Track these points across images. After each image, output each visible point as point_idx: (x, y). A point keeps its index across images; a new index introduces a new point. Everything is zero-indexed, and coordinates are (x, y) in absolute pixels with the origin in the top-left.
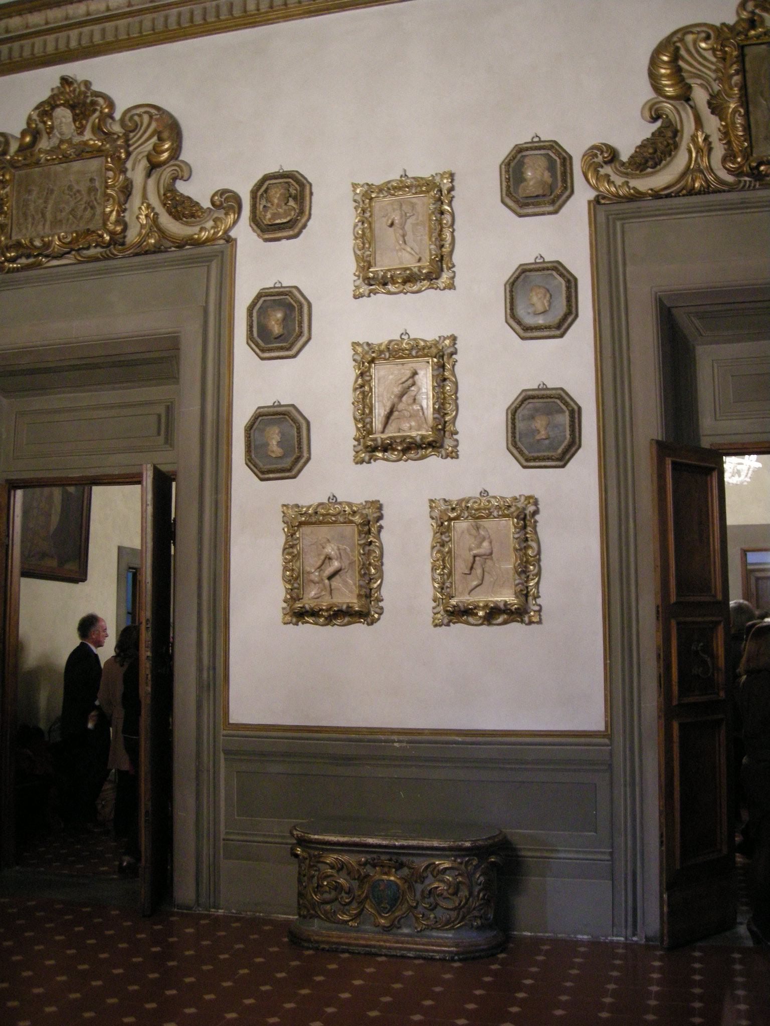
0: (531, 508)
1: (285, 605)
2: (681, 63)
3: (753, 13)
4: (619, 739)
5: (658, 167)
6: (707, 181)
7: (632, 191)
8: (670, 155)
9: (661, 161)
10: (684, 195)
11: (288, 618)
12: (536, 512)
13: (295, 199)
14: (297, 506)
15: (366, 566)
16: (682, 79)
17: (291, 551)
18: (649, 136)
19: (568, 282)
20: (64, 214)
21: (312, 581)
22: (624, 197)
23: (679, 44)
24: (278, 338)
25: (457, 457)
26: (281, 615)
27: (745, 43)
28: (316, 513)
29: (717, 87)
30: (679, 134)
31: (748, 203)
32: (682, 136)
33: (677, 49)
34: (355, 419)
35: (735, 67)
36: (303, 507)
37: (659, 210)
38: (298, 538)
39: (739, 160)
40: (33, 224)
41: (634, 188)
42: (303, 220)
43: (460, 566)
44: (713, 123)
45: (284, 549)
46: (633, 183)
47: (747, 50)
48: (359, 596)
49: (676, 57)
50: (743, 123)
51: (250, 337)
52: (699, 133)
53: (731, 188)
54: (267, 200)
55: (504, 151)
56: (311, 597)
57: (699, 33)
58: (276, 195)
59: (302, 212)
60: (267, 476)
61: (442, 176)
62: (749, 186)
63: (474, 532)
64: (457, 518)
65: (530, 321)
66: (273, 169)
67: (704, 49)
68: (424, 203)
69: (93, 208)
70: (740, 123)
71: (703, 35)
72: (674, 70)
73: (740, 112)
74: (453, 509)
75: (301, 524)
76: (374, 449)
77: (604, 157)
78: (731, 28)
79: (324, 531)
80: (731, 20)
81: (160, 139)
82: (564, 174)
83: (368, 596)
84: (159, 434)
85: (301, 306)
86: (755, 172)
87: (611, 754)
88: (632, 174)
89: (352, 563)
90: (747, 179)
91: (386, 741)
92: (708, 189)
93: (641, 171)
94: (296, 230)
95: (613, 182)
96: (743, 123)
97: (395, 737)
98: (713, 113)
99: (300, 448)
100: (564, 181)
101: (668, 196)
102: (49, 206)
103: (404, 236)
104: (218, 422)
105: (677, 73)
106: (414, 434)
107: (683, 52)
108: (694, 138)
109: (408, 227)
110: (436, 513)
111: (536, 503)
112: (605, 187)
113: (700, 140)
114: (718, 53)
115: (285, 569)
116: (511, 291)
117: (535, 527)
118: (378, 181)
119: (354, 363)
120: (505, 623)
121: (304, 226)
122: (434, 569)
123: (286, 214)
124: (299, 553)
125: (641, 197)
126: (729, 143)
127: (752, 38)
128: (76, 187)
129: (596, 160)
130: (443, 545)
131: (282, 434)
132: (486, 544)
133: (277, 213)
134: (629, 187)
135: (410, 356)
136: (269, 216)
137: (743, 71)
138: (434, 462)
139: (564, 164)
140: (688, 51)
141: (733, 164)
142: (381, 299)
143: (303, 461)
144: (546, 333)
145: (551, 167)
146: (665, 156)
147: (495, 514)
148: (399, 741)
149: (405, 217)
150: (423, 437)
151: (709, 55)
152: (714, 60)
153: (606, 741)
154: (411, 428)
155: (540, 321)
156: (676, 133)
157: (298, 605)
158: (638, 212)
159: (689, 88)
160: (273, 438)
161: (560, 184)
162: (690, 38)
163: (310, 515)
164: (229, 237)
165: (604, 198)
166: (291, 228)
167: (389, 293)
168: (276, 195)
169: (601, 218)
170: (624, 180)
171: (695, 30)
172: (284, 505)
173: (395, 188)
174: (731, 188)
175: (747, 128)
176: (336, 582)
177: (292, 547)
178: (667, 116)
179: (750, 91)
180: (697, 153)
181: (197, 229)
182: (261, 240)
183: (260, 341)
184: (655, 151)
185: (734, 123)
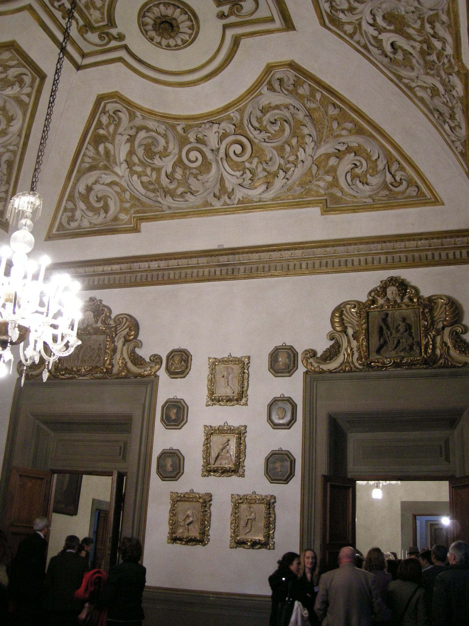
0: (273, 500)
1: (169, 535)
2: (343, 317)
3: (374, 297)
6: (351, 368)
8: (337, 356)
9: (333, 358)
11: (169, 541)
12: (275, 502)
13: (185, 361)
14: (177, 493)
15: (203, 521)
16: (343, 324)
17: (173, 512)
18: (328, 347)
19: (293, 406)
20: (87, 358)
21: (181, 526)
22: (317, 372)
23: (343, 309)
24: (174, 421)
25: (244, 477)
26: (167, 539)
28: (184, 496)
33: (343, 311)
34: (203, 458)
36: (179, 493)
38: (176, 507)
40: (73, 360)
41: (322, 369)
42: (187, 371)
43: (242, 523)
44: (354, 344)
45: (170, 511)
46: (321, 366)
48: (200, 533)
51: (162, 419)
53: (361, 370)
55: (271, 349)
56: (180, 532)
58: (177, 359)
59: (187, 368)
60: (165, 479)
61: (245, 357)
63: (249, 509)
64: (242, 503)
65: (277, 421)
66: (176, 347)
68: (236, 369)
69: (100, 357)
71: (353, 306)
74: (241, 499)
75: (178, 501)
76: (210, 471)
79: (187, 505)
81: (130, 330)
82: (294, 361)
83: (204, 533)
84: (120, 455)
85: (184, 408)
86: (370, 365)
89: (198, 519)
91: (208, 597)
94: (184, 375)
97: (211, 595)
99: (180, 468)
100: (294, 364)
101: (335, 372)
102: (81, 353)
103: (228, 382)
104: (146, 454)
105: (342, 320)
106: (226, 466)
107: (345, 312)
108: (346, 350)
109: (230, 378)
110: (234, 500)
111: (275, 498)
112: (309, 367)
115: (170, 519)
116: (270, 409)
117: (274, 509)
118: (219, 357)
119: (204, 434)
120: (259, 548)
121: (188, 373)
122: (231, 524)
123: (181, 368)
124: (176, 513)
126: (360, 352)
128: (93, 347)
129: (307, 356)
130: (236, 514)
131: (173, 461)
132: (253, 514)
133: (177, 366)
134: (319, 368)
135: (227, 433)
136: (173, 368)
137: (368, 322)
138: (234, 478)
139: (294, 357)
140: (347, 312)
142: (217, 407)
143: (180, 474)
144: (283, 427)
145: (289, 357)
147: (258, 502)
148: (213, 597)
149: (229, 374)
150: (230, 468)
151: (355, 314)
154: (225, 463)
155: (281, 422)
157: (174, 535)
159: (346, 328)
160: (169, 463)
161: (292, 365)
163: (182, 497)
164: (156, 375)
165: (309, 372)
166: (182, 374)
167: (220, 405)
168: (177, 359)
169: (308, 380)
170: (318, 365)
172: (171, 492)
173: (226, 361)
174: (361, 370)
175: (368, 347)
176: (191, 527)
177: (173, 510)
178: (337, 339)
179: (370, 330)
181: (143, 370)
182: (169, 378)
183: (166, 421)
185: (362, 344)
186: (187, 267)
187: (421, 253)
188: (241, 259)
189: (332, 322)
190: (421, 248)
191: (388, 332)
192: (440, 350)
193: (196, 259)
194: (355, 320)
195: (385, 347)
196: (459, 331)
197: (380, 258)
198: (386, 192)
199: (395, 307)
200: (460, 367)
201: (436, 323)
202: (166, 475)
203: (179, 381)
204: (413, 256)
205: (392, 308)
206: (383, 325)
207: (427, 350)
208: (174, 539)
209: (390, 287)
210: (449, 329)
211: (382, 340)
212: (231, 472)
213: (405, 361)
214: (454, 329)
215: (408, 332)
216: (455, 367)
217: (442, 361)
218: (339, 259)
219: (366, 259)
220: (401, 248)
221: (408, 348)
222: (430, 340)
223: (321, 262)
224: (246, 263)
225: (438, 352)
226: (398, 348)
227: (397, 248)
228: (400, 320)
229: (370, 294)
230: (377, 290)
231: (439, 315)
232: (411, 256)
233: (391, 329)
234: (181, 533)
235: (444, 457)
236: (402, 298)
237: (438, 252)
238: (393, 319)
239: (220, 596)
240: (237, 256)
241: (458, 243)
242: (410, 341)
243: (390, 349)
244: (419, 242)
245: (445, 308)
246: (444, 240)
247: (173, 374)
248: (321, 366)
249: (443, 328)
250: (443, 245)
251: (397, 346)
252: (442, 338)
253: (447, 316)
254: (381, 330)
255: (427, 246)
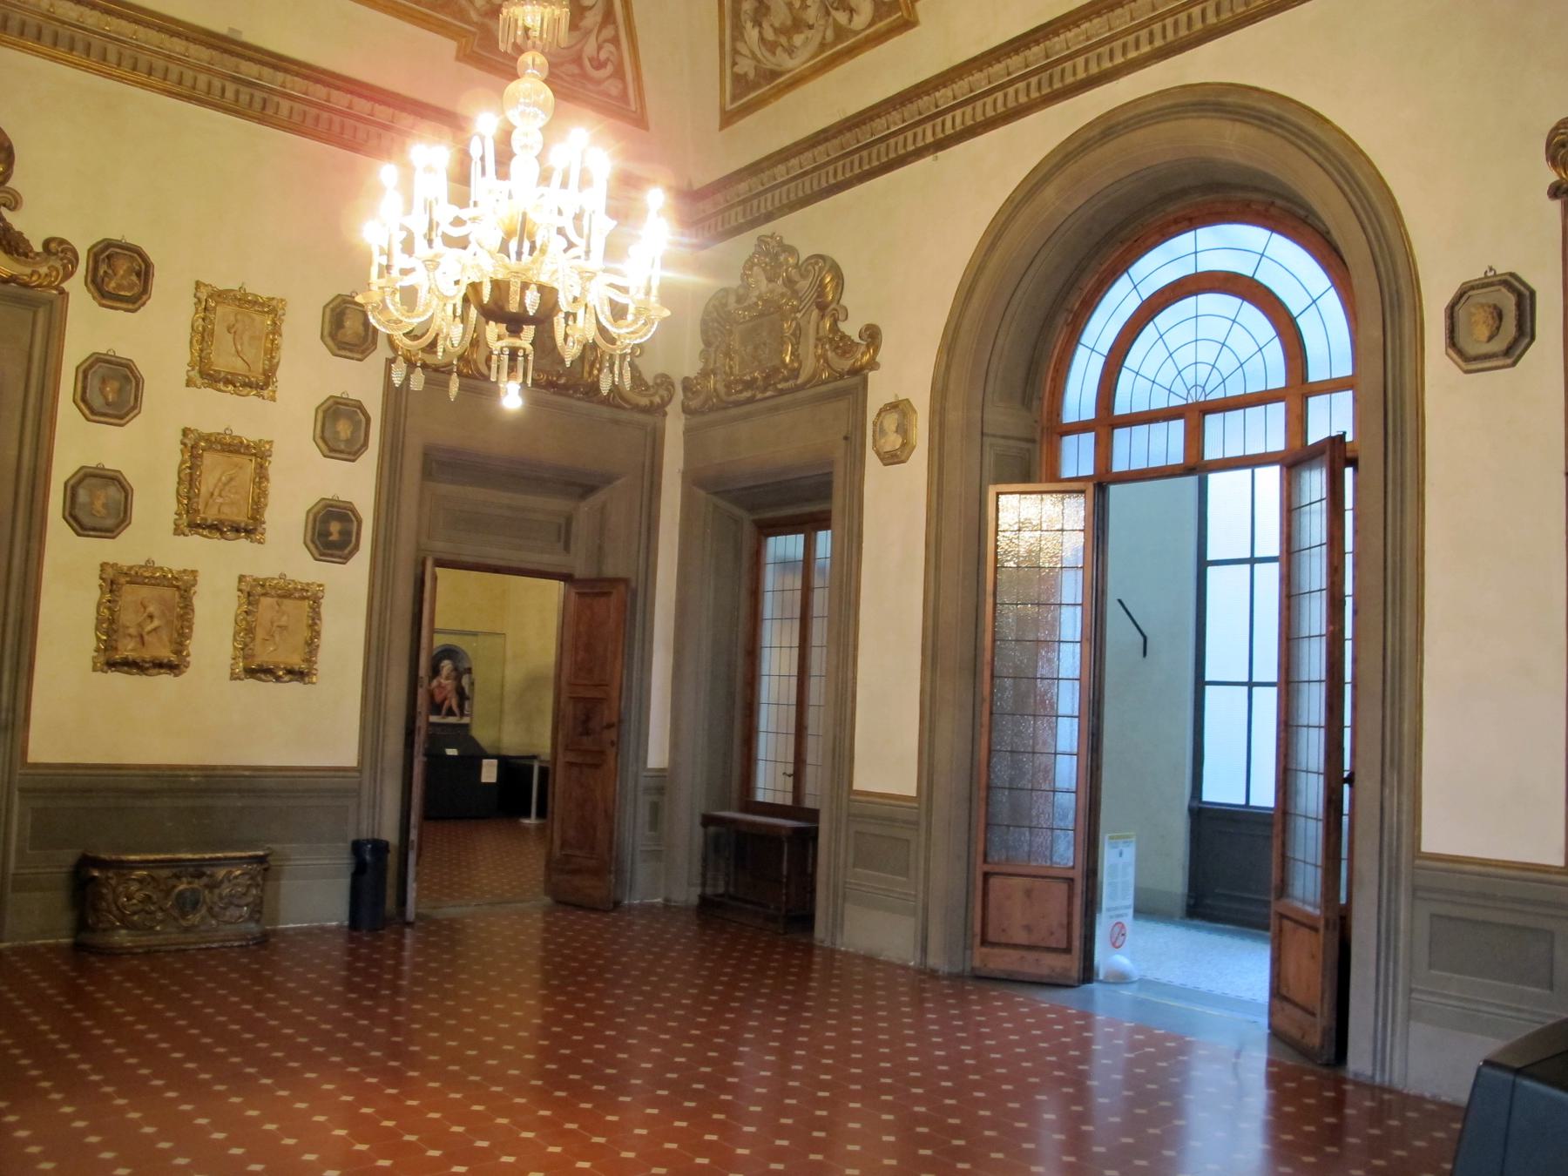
4: (367, 773)
13: (138, 274)
43: (260, 634)
54: (109, 266)
56: (128, 649)
60: (86, 533)
63: (277, 607)
79: (144, 592)
87: (360, 784)
101: (443, 372)
136: (113, 284)
138: (243, 544)
148: (196, 776)
153: (357, 774)
166: (134, 303)
181: (28, 271)
182: (95, 304)
186: (157, 53)
188: (289, 85)
193: (184, 43)
198: (576, 70)
202: (80, 525)
203: (119, 316)
208: (113, 662)
212: (204, 529)
224: (297, 97)
234: (132, 650)
235: (562, 543)
239: (208, 773)
240: (280, 76)
247: (103, 292)
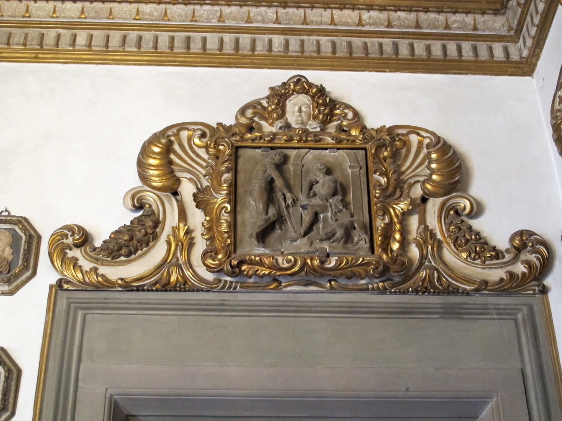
2: (172, 156)
3: (251, 119)
5: (133, 256)
6: (184, 276)
7: (100, 279)
8: (147, 245)
9: (136, 250)
10: (157, 290)
16: (172, 172)
19: (9, 371)
22: (92, 284)
23: (173, 138)
27: (240, 144)
29: (206, 183)
30: (160, 225)
31: (227, 305)
32: (163, 229)
33: (170, 143)
35: (226, 164)
37: (127, 303)
39: (220, 256)
41: (103, 276)
46: (103, 270)
47: (241, 152)
49: (168, 149)
50: (229, 220)
52: (181, 225)
53: (210, 287)
57: (194, 130)
62: (230, 287)
67: (199, 147)
70: (225, 220)
71: (199, 132)
72: (164, 161)
73: (227, 208)
77: (74, 239)
78: (228, 129)
80: (229, 121)
82: (28, 252)
86: (237, 270)
88: (103, 260)
90: (229, 279)
92: (184, 285)
93: (113, 258)
95: (80, 267)
96: (229, 220)
98: (198, 206)
100: (26, 260)
101: (139, 289)
107: (176, 147)
112: (70, 274)
113: (182, 233)
114: (211, 150)
125: (108, 287)
127: (247, 140)
129: (65, 241)
137: (235, 171)
139: (29, 242)
141: (213, 260)
146: (141, 245)
151: (202, 152)
152: (206, 157)
156: (157, 223)
158: (104, 303)
159: (178, 181)
161: (20, 262)
162: (184, 134)
165: (68, 282)
169: (62, 305)
171: (191, 127)
174: (210, 287)
175: (233, 225)
178: (150, 206)
180: (177, 245)
184: (131, 239)
185: (219, 218)
187: (367, 40)
189: (141, 165)
190: (367, 28)
191: (288, 195)
192: (419, 246)
194: (201, 165)
195: (279, 231)
196: (465, 208)
197: (270, 41)
199: (307, 141)
200: (467, 293)
201: (406, 186)
204: (350, 44)
205: (299, 141)
206: (275, 174)
207: (388, 244)
209: (295, 95)
210: (439, 201)
211: (272, 211)
213: (333, 264)
214: (452, 202)
215: (339, 197)
216: (456, 291)
217: (423, 274)
218: (172, 34)
219: (237, 40)
220: (321, 23)
221: (339, 234)
222: (396, 220)
223: (125, 37)
225: (414, 252)
226: (313, 233)
227: (312, 22)
228: (320, 170)
229: (242, 111)
230: (260, 104)
231: (414, 171)
232: (344, 44)
233: (297, 191)
236: (325, 123)
237: (407, 41)
238: (300, 168)
241: (455, 25)
242: (345, 219)
243: (292, 233)
244: (366, 15)
245: (429, 154)
246: (422, 15)
248: (103, 270)
249: (424, 200)
250: (421, 28)
251: (309, 230)
252: (422, 221)
253: (433, 172)
254: (270, 185)
255: (382, 24)
